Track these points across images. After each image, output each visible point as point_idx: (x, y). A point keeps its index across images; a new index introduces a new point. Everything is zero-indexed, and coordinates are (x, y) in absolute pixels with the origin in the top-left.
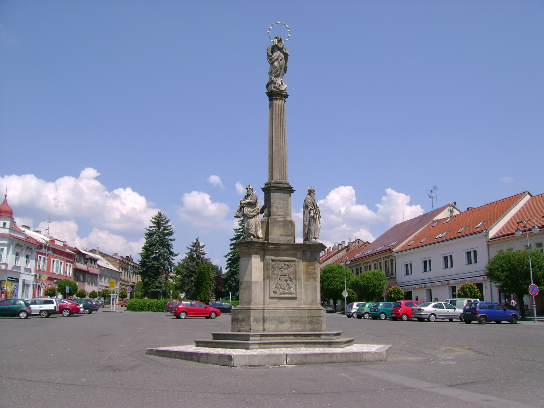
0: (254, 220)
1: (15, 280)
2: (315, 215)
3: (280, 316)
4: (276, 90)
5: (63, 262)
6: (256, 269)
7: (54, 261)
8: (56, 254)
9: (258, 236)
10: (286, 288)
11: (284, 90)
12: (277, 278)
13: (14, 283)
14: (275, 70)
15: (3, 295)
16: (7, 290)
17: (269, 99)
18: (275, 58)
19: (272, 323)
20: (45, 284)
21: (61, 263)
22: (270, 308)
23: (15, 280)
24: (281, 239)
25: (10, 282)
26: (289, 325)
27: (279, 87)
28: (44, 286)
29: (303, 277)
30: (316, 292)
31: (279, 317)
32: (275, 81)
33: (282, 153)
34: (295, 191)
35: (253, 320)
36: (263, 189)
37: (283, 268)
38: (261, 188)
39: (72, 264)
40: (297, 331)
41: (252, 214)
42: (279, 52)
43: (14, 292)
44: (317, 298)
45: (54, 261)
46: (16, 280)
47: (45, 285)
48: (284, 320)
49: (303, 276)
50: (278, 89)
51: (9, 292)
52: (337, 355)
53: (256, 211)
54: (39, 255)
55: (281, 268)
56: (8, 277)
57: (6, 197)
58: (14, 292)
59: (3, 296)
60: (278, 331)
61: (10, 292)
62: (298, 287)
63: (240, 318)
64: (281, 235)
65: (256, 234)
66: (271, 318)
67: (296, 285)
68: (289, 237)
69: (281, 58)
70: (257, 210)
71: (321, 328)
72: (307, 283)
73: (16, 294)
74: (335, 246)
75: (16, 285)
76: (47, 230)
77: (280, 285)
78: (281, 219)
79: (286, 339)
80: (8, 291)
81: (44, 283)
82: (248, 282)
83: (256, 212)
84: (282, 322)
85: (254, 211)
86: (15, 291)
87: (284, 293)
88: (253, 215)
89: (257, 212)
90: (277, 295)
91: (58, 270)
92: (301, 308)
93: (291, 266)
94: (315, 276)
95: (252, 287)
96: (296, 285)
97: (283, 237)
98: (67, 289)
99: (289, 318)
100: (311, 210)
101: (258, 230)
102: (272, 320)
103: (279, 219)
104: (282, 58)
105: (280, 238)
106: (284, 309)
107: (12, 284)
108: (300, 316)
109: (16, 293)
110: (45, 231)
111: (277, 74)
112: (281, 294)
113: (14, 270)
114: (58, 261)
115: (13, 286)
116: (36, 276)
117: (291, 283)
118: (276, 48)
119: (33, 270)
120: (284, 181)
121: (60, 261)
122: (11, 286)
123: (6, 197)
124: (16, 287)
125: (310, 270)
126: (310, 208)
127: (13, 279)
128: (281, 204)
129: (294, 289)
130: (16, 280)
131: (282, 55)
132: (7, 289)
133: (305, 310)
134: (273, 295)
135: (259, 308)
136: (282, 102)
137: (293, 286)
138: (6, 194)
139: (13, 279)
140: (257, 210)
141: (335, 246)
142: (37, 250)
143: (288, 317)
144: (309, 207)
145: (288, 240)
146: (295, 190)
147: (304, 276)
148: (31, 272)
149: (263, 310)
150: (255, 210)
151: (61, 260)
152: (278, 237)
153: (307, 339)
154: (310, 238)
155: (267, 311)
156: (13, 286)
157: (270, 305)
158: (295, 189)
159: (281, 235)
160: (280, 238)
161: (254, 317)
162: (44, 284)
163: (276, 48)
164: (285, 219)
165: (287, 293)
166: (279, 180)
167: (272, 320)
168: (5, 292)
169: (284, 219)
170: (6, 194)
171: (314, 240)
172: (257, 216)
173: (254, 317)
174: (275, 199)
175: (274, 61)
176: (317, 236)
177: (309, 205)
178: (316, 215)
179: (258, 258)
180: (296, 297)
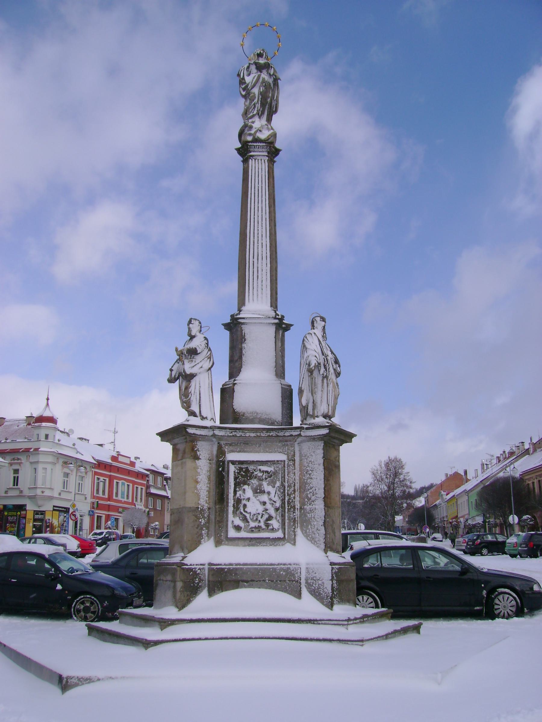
1: (63, 509)
5: (131, 485)
7: (117, 483)
13: (63, 514)
15: (48, 529)
16: (53, 524)
17: (242, 159)
21: (128, 485)
23: (63, 509)
28: (74, 517)
34: (291, 328)
35: (182, 588)
39: (144, 488)
43: (63, 525)
45: (117, 483)
46: (65, 510)
51: (56, 525)
54: (96, 477)
56: (54, 506)
58: (63, 525)
59: (49, 531)
61: (57, 525)
73: (67, 529)
74: (511, 449)
75: (66, 517)
76: (112, 442)
80: (54, 525)
86: (65, 525)
90: (243, 534)
91: (124, 495)
95: (186, 520)
107: (59, 516)
109: (66, 526)
110: (110, 444)
113: (62, 496)
115: (62, 518)
121: (126, 483)
122: (59, 517)
124: (65, 519)
127: (60, 509)
130: (65, 510)
132: (53, 522)
138: (48, 397)
139: (60, 509)
141: (511, 449)
142: (93, 469)
148: (86, 498)
156: (62, 518)
158: (293, 324)
168: (50, 526)
170: (48, 397)
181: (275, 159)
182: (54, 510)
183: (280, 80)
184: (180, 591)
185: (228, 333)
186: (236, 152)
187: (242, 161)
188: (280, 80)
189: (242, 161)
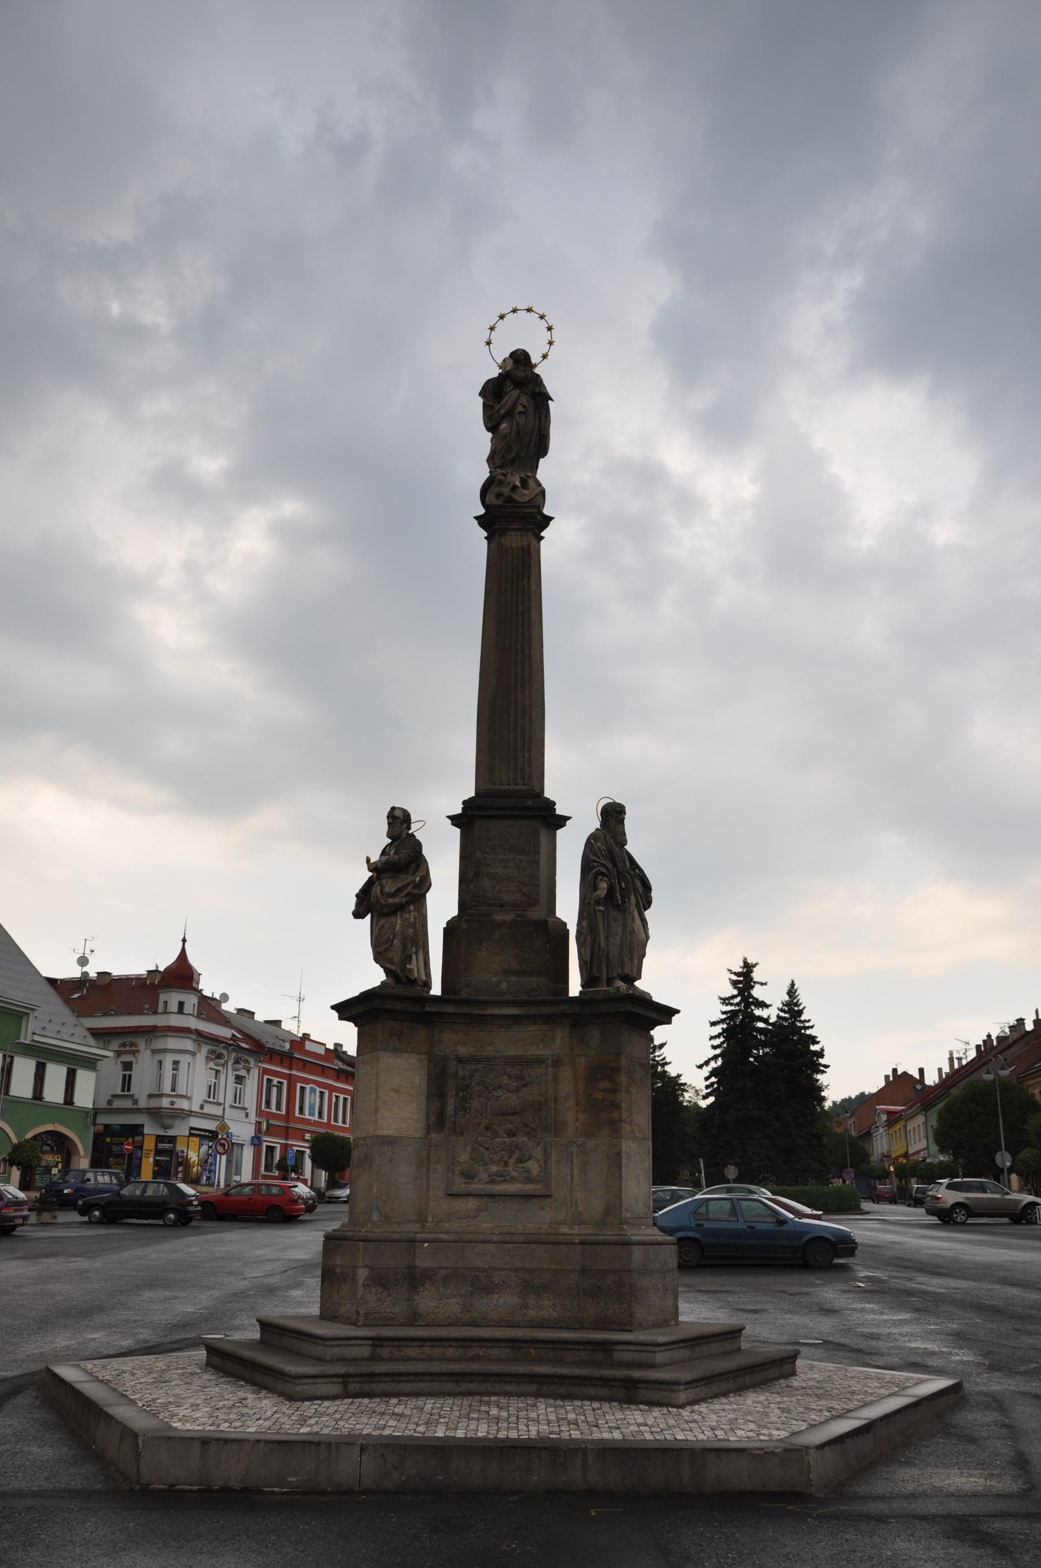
0: (399, 922)
1: (207, 1134)
2: (618, 895)
3: (478, 1264)
4: (504, 503)
5: (327, 1092)
6: (397, 1091)
7: (303, 1089)
8: (310, 1072)
9: (407, 977)
10: (512, 1161)
11: (528, 502)
12: (479, 1124)
13: (207, 1142)
14: (502, 445)
15: (180, 1169)
16: (190, 1158)
17: (485, 534)
18: (502, 412)
19: (449, 1292)
20: (224, 1144)
21: (322, 1093)
22: (442, 1236)
23: (207, 1134)
24: (504, 985)
25: (197, 1140)
26: (516, 1300)
27: (511, 494)
28: (222, 1149)
29: (577, 1120)
30: (621, 1176)
31: (478, 1269)
32: (501, 477)
33: (520, 697)
34: (568, 823)
35: (366, 1279)
36: (455, 820)
37: (500, 1087)
38: (449, 817)
39: (349, 1097)
40: (542, 1325)
41: (390, 901)
42: (516, 392)
44: (621, 1200)
45: (303, 1089)
46: (211, 1135)
47: (224, 1147)
48: (496, 1281)
49: (572, 1117)
50: (510, 500)
51: (194, 1162)
52: (585, 1454)
53: (409, 889)
54: (266, 1077)
55: (495, 1089)
56: (191, 1128)
57: (184, 945)
58: (206, 1162)
59: (181, 1172)
60: (473, 1324)
61: (196, 1162)
62: (554, 1158)
63: (338, 1270)
64: (506, 972)
65: (404, 969)
66: (442, 1273)
67: (546, 1153)
68: (533, 979)
69: (520, 408)
70: (411, 887)
71: (631, 1315)
72: (590, 1143)
73: (213, 1168)
75: (211, 1147)
76: (295, 1017)
77: (487, 1149)
78: (508, 917)
79: (478, 1358)
80: (192, 1160)
81: (223, 1142)
82: (368, 1140)
83: (406, 895)
84: (488, 1290)
85: (399, 890)
86: (210, 1161)
87: (505, 1179)
88: (396, 904)
89: (409, 894)
90: (476, 1186)
91: (314, 1109)
92: (559, 1235)
93: (532, 1082)
94: (616, 1116)
96: (546, 1153)
97: (514, 979)
98: (290, 1155)
99: (514, 1274)
100: (600, 877)
101: (411, 957)
102: (446, 1279)
103: (498, 917)
104: (524, 407)
105: (499, 983)
106: (495, 1238)
107: (201, 1145)
108: (553, 1267)
109: (211, 1164)
111: (510, 457)
112: (493, 1182)
114: (313, 1090)
115: (204, 1148)
116: (258, 1124)
117: (529, 1143)
118: (508, 383)
119: (252, 1111)
120: (524, 787)
121: (318, 1090)
122: (199, 1148)
123: (184, 945)
124: (210, 1152)
125: (600, 1096)
126: (595, 870)
127: (202, 1133)
128: (511, 864)
129: (542, 1164)
130: (211, 1135)
131: (524, 399)
132: (189, 1157)
133: (573, 1243)
134: (459, 1185)
135: (397, 1236)
136: (524, 538)
137: (538, 1152)
138: (184, 937)
139: (202, 1133)
140: (411, 887)
142: (260, 1064)
143: (511, 1269)
144: (594, 867)
145: (531, 990)
146: (569, 818)
147: (581, 1116)
148: (247, 1115)
149: (413, 1241)
150: (405, 886)
151: (320, 1087)
152: (494, 979)
153: (561, 1362)
154: (604, 975)
155: (426, 1245)
156: (204, 1148)
157: (446, 1225)
159: (506, 972)
160: (499, 983)
161: (372, 1269)
162: (221, 1145)
163: (508, 383)
164: (521, 916)
165: (513, 1180)
166: (507, 787)
167: (446, 1279)
169: (517, 916)
170: (184, 937)
171: (620, 984)
172: (412, 908)
173: (372, 1269)
174: (488, 850)
175: (498, 419)
176: (632, 971)
177: (595, 861)
178: (622, 896)
179: (407, 1055)
180: (549, 1194)
181: (542, 534)
182: (191, 1135)
183: (552, 400)
184: (364, 1285)
185: (457, 831)
186: (476, 522)
187: (486, 538)
188: (552, 400)
189: (486, 538)
